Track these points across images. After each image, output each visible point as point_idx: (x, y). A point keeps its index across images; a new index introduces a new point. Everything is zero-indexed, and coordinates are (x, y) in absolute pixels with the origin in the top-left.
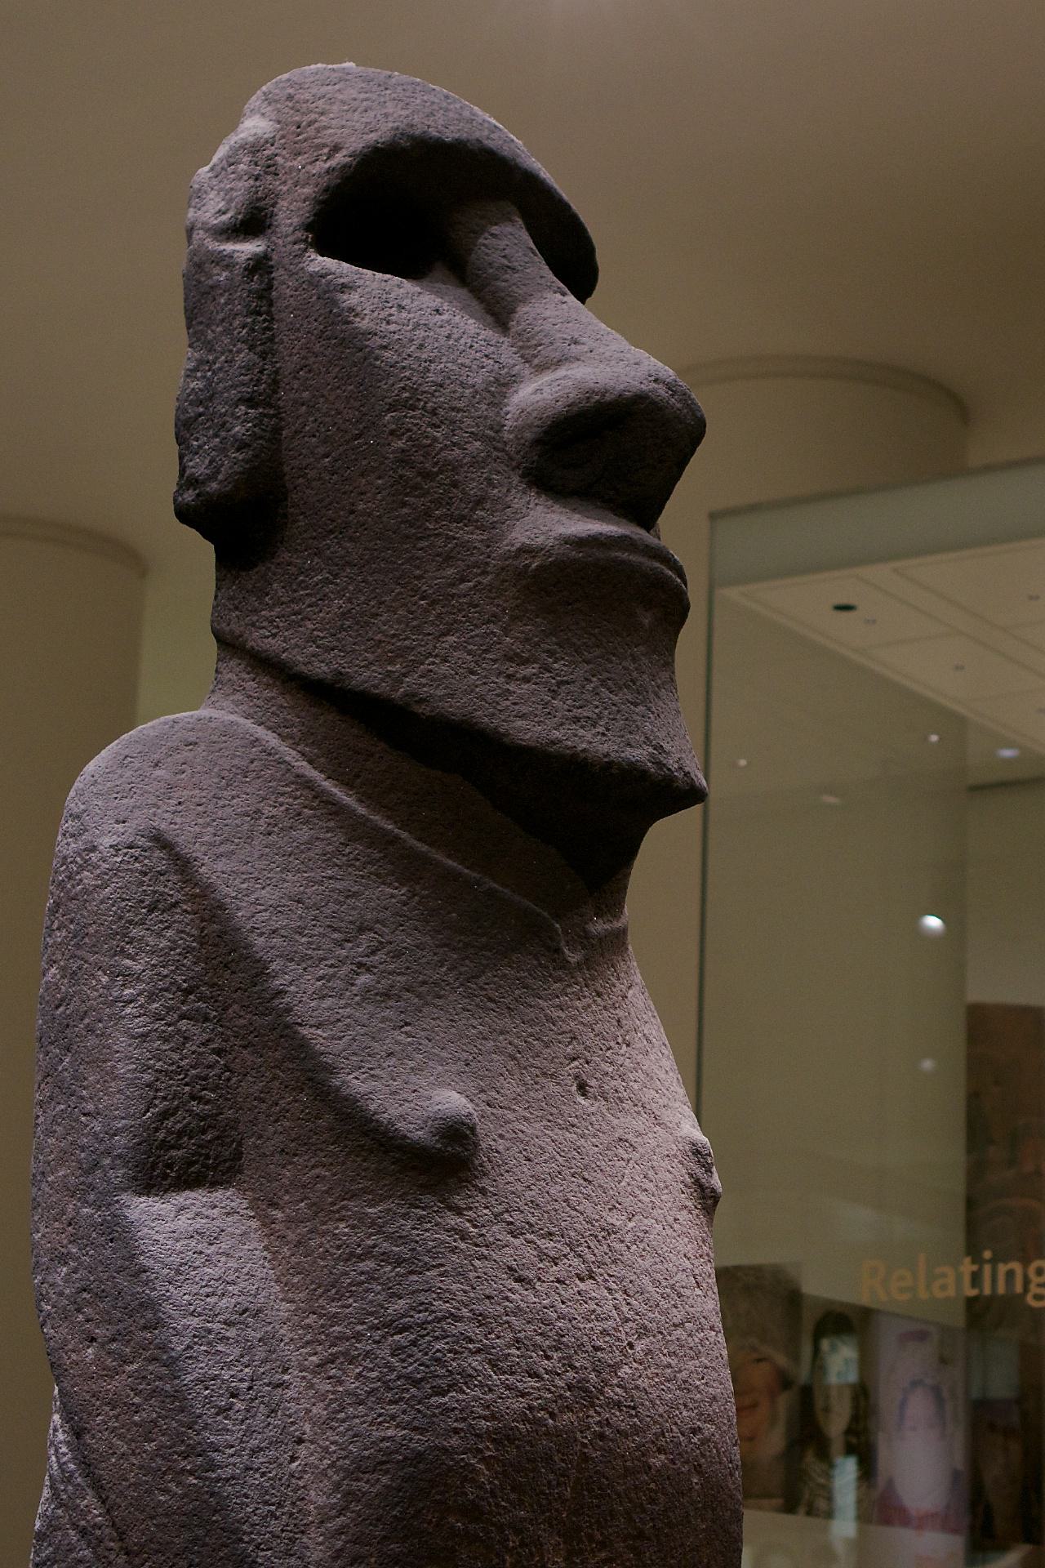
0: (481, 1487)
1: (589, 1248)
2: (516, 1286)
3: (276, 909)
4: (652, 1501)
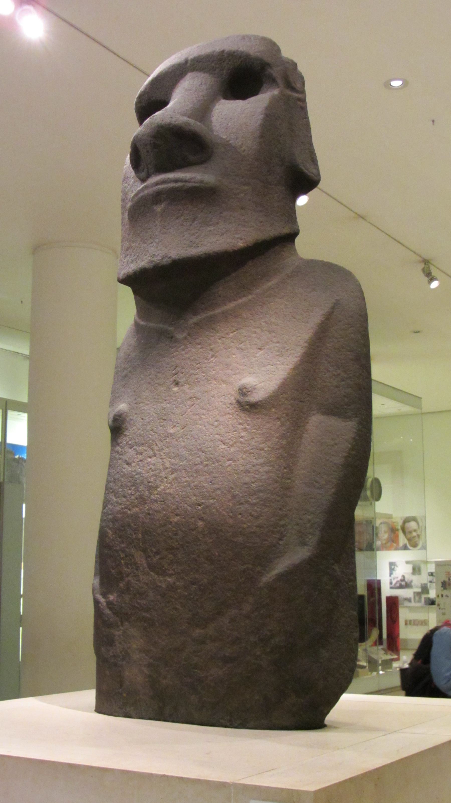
1: (157, 445)
4: (176, 534)
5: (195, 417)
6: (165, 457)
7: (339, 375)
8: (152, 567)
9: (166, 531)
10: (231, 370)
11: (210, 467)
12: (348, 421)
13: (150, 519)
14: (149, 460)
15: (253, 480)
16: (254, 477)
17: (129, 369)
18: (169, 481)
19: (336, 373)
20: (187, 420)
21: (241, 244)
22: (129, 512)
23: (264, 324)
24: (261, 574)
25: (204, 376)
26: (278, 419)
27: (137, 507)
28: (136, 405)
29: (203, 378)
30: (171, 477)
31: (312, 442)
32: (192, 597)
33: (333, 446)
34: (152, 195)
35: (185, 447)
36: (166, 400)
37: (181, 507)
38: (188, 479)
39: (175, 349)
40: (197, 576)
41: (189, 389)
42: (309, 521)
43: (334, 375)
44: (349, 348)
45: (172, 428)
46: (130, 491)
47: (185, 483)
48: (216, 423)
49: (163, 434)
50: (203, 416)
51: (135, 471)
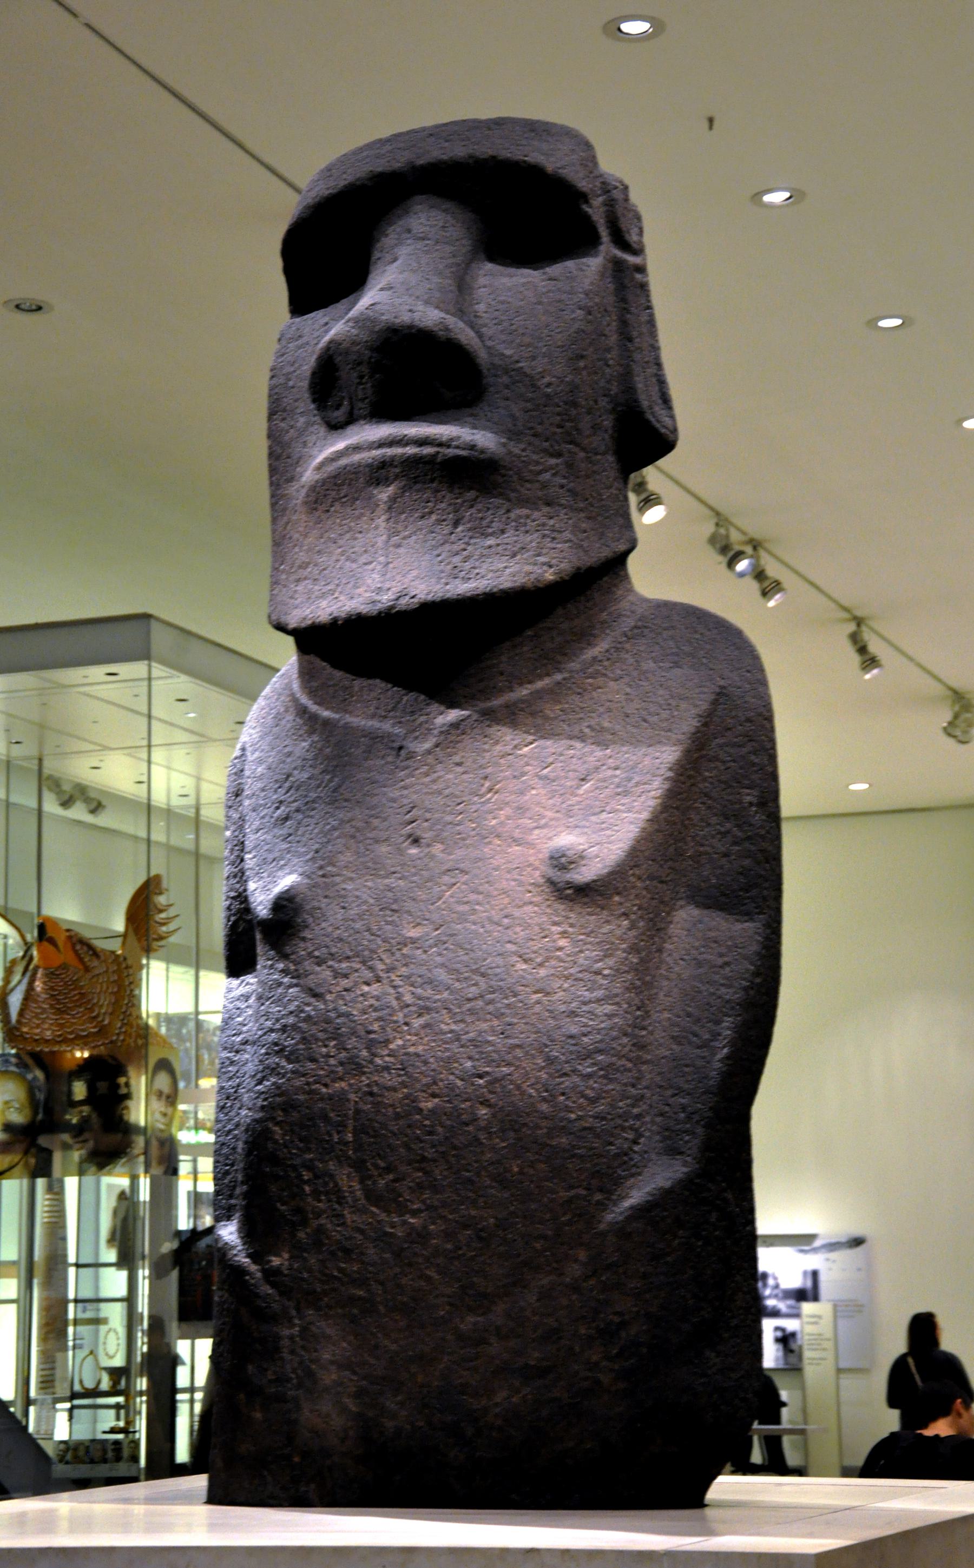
0: (276, 1142)
1: (381, 960)
2: (312, 1000)
3: (260, 778)
4: (430, 1133)
5: (461, 908)
6: (401, 983)
7: (728, 832)
8: (373, 1197)
9: (409, 1126)
10: (530, 819)
11: (499, 1005)
12: (746, 921)
13: (372, 1103)
14: (366, 988)
15: (584, 1030)
16: (586, 1026)
17: (296, 804)
18: (413, 1031)
19: (723, 829)
20: (445, 912)
21: (550, 576)
22: (324, 1090)
23: (587, 730)
24: (602, 1206)
25: (474, 829)
26: (625, 914)
27: (341, 1079)
28: (324, 879)
29: (473, 833)
30: (417, 1023)
31: (682, 959)
32: (460, 1252)
33: (721, 967)
34: (369, 466)
35: (443, 965)
36: (394, 873)
37: (442, 1080)
38: (454, 1027)
39: (407, 771)
40: (473, 1213)
41: (443, 851)
42: (684, 1108)
43: (720, 833)
44: (747, 782)
45: (414, 927)
46: (324, 1050)
47: (449, 1035)
48: (506, 921)
49: (393, 938)
50: (477, 907)
51: (335, 1009)
